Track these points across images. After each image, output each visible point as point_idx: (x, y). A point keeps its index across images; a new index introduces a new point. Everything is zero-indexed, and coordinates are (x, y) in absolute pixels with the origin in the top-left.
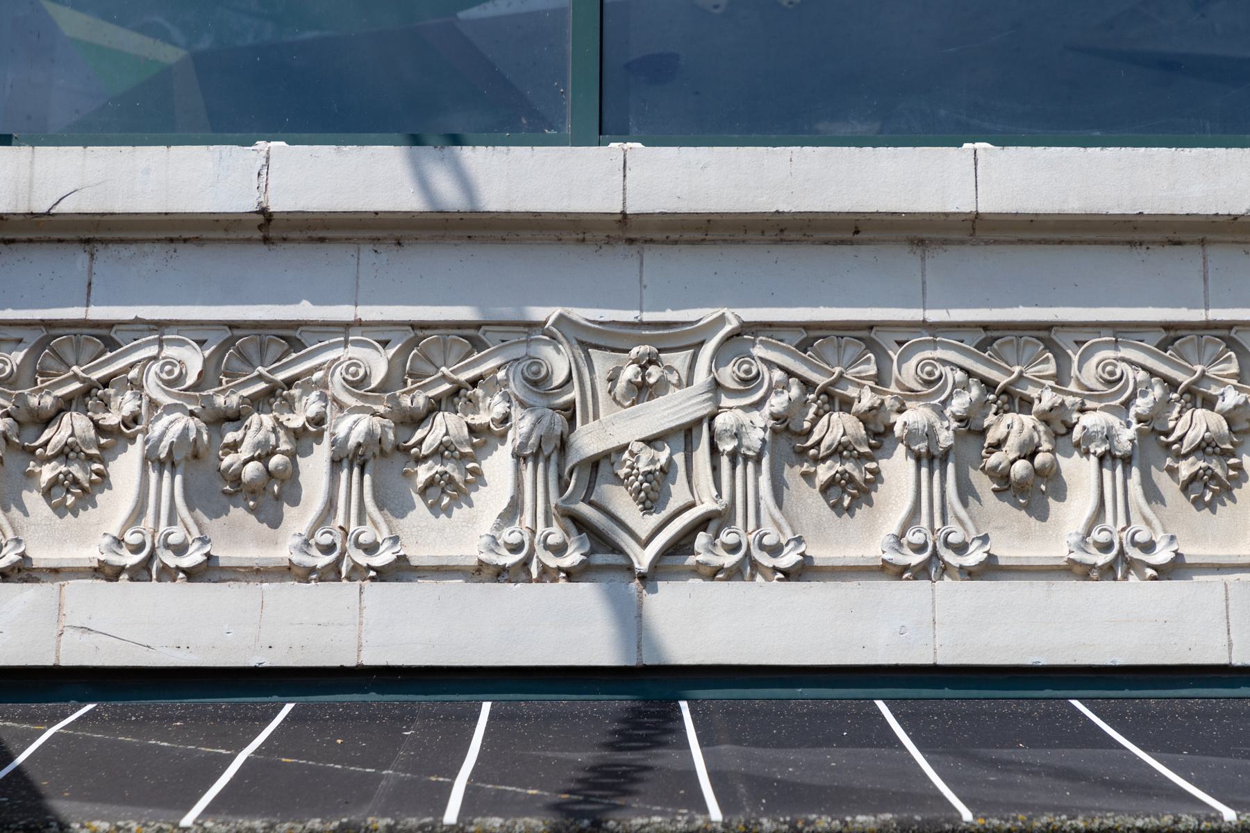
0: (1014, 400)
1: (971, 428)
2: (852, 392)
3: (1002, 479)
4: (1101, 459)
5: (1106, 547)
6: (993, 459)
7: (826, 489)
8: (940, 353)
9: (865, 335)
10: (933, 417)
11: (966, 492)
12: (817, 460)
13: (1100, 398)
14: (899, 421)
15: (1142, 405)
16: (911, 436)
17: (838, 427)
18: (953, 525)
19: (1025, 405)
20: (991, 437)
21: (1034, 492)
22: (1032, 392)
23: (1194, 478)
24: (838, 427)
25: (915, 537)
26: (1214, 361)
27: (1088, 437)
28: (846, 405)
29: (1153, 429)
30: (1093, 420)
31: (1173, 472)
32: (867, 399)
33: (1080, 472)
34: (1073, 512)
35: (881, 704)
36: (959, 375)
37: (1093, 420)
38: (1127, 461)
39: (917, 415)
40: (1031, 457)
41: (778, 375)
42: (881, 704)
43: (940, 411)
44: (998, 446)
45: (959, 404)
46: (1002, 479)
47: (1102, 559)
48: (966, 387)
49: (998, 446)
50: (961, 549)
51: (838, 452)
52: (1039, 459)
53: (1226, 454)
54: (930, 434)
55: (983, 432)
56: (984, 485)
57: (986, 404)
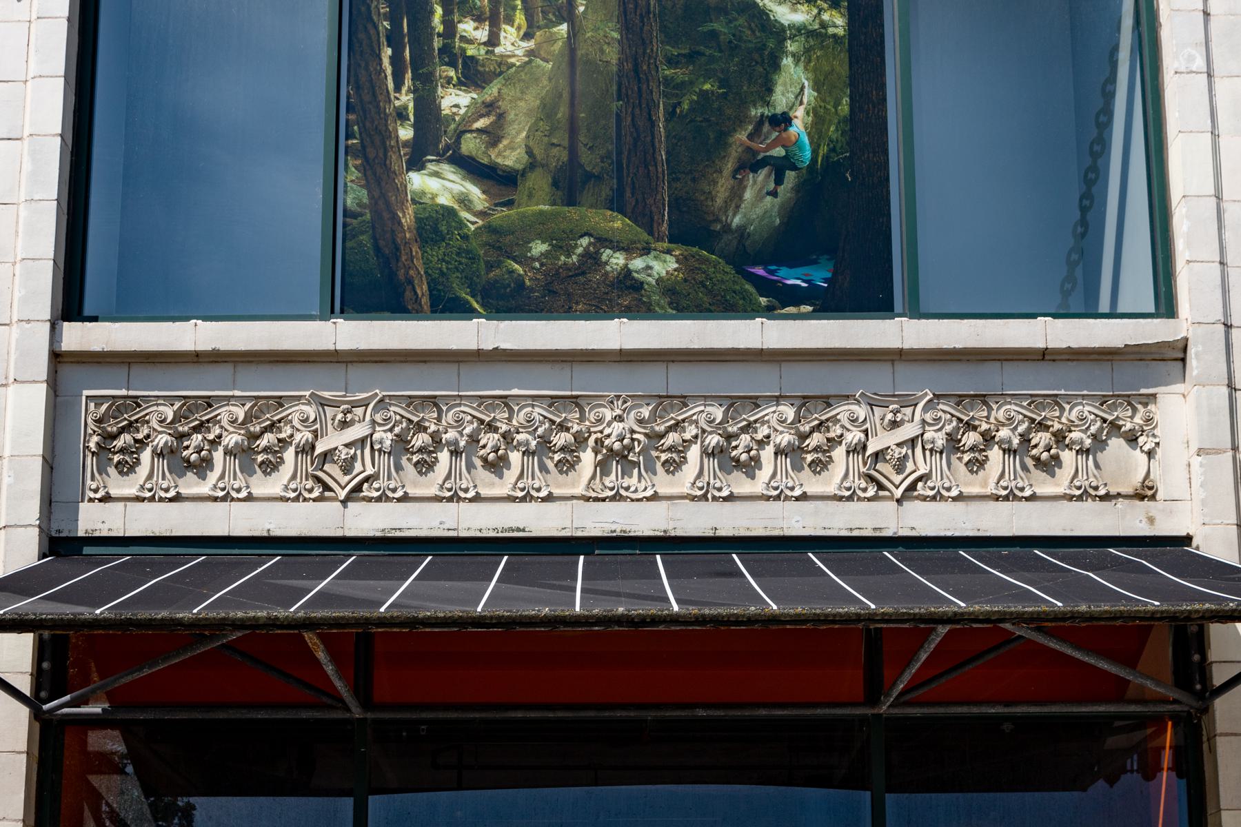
0: (492, 428)
1: (474, 439)
2: (427, 424)
3: (485, 460)
4: (524, 453)
5: (522, 490)
6: (482, 452)
7: (416, 465)
8: (463, 408)
9: (433, 401)
10: (457, 435)
11: (470, 466)
12: (413, 453)
13: (525, 427)
14: (444, 436)
15: (540, 431)
16: (448, 443)
17: (420, 440)
18: (464, 481)
19: (496, 430)
20: (482, 443)
21: (497, 465)
22: (499, 424)
23: (560, 461)
24: (420, 440)
25: (448, 485)
26: (570, 412)
27: (519, 444)
28: (425, 429)
29: (545, 442)
30: (521, 437)
31: (552, 459)
32: (433, 428)
33: (515, 457)
34: (511, 475)
35: (734, 556)
36: (469, 418)
37: (521, 437)
38: (533, 453)
39: (451, 435)
40: (496, 451)
41: (398, 417)
42: (734, 556)
43: (461, 433)
44: (484, 447)
45: (468, 430)
46: (485, 460)
47: (520, 494)
48: (472, 423)
49: (484, 447)
50: (466, 490)
51: (421, 450)
52: (500, 452)
53: (573, 451)
54: (456, 443)
55: (478, 441)
56: (478, 463)
57: (481, 430)
